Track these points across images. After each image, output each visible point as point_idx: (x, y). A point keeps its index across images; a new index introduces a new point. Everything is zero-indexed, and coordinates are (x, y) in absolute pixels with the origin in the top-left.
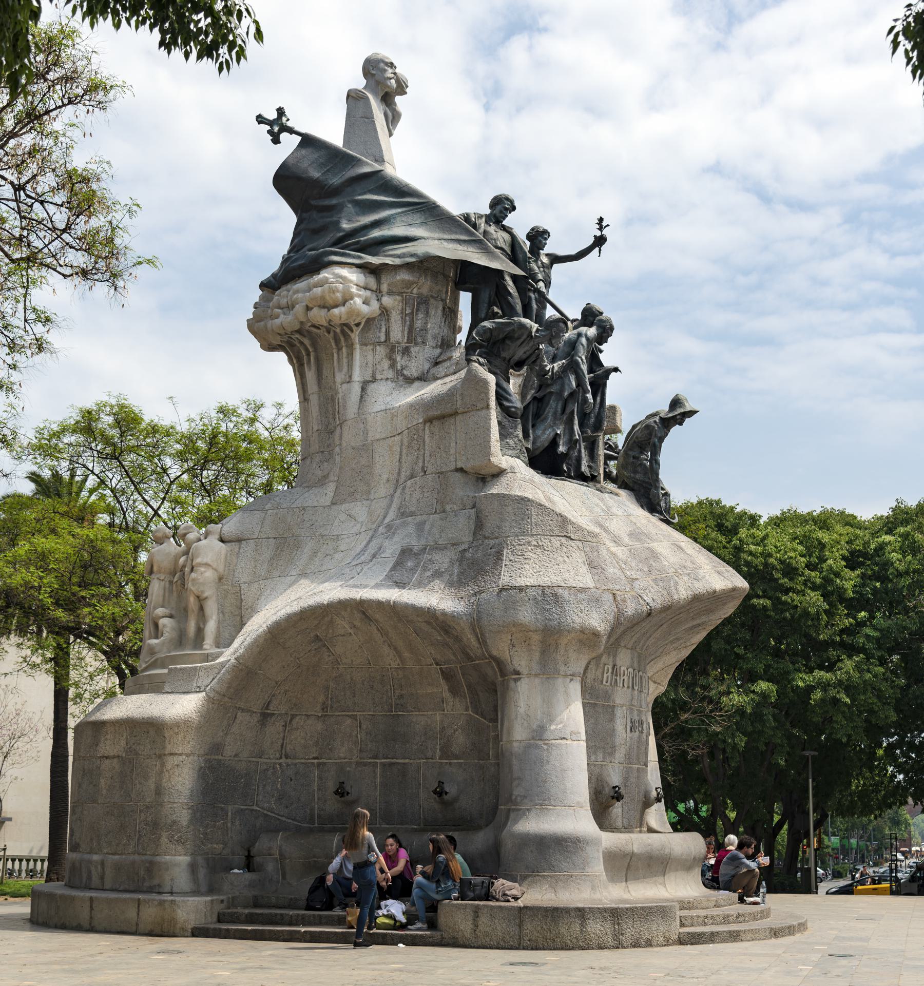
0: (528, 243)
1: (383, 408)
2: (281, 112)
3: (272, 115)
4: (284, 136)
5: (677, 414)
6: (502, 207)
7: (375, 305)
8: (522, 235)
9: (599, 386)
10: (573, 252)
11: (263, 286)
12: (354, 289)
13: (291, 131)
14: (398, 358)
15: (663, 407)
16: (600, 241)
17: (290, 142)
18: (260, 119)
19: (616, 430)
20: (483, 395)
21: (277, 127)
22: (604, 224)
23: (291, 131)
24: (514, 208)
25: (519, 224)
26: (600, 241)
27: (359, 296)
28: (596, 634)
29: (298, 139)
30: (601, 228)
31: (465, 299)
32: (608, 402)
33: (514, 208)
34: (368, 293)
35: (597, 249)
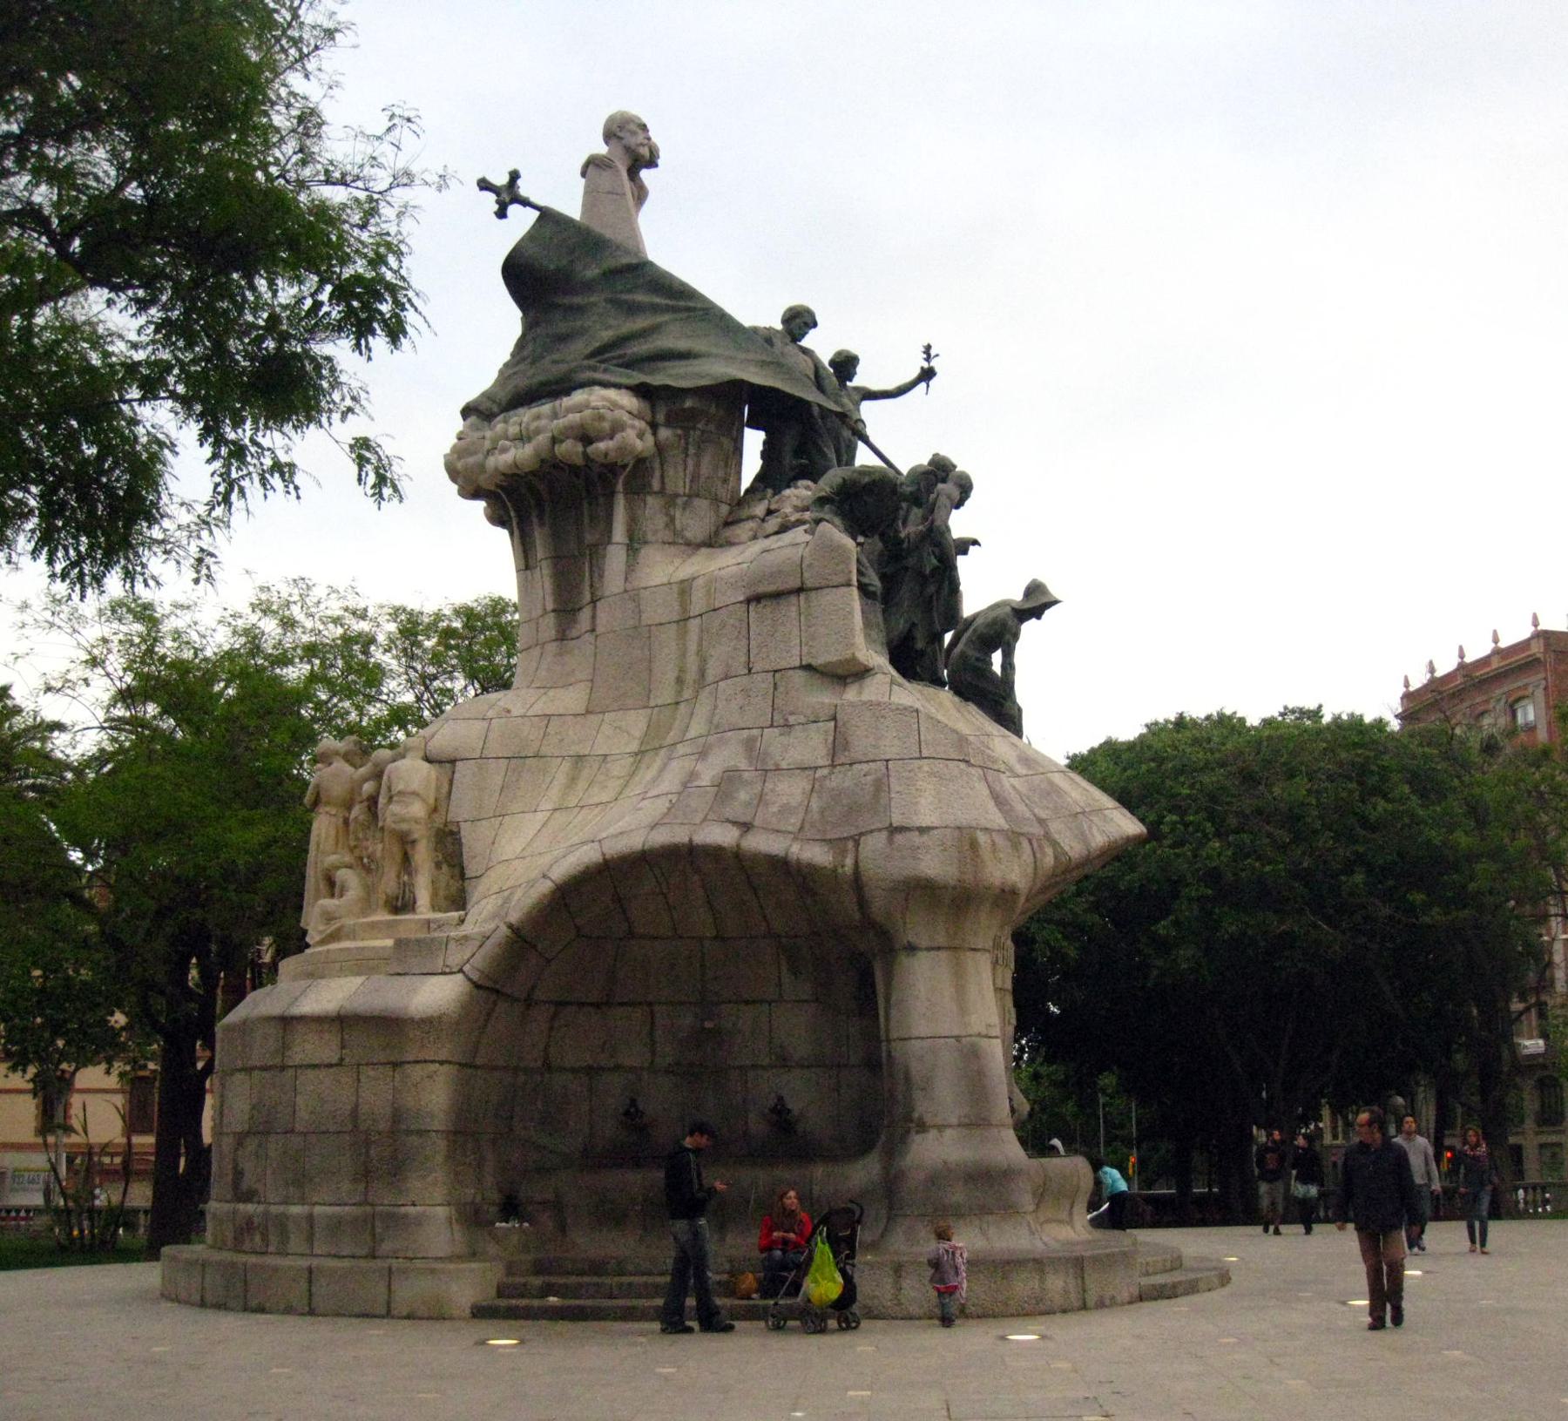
1: (665, 580)
2: (514, 176)
3: (501, 180)
4: (514, 209)
5: (1036, 603)
6: (799, 321)
7: (650, 439)
8: (825, 357)
10: (890, 385)
11: (467, 412)
12: (626, 417)
13: (525, 203)
15: (1016, 595)
16: (927, 375)
17: (521, 220)
18: (484, 185)
21: (507, 196)
22: (933, 353)
23: (525, 203)
24: (815, 325)
25: (822, 344)
26: (927, 375)
27: (633, 427)
28: (1014, 892)
29: (536, 214)
30: (928, 359)
31: (754, 441)
33: (815, 325)
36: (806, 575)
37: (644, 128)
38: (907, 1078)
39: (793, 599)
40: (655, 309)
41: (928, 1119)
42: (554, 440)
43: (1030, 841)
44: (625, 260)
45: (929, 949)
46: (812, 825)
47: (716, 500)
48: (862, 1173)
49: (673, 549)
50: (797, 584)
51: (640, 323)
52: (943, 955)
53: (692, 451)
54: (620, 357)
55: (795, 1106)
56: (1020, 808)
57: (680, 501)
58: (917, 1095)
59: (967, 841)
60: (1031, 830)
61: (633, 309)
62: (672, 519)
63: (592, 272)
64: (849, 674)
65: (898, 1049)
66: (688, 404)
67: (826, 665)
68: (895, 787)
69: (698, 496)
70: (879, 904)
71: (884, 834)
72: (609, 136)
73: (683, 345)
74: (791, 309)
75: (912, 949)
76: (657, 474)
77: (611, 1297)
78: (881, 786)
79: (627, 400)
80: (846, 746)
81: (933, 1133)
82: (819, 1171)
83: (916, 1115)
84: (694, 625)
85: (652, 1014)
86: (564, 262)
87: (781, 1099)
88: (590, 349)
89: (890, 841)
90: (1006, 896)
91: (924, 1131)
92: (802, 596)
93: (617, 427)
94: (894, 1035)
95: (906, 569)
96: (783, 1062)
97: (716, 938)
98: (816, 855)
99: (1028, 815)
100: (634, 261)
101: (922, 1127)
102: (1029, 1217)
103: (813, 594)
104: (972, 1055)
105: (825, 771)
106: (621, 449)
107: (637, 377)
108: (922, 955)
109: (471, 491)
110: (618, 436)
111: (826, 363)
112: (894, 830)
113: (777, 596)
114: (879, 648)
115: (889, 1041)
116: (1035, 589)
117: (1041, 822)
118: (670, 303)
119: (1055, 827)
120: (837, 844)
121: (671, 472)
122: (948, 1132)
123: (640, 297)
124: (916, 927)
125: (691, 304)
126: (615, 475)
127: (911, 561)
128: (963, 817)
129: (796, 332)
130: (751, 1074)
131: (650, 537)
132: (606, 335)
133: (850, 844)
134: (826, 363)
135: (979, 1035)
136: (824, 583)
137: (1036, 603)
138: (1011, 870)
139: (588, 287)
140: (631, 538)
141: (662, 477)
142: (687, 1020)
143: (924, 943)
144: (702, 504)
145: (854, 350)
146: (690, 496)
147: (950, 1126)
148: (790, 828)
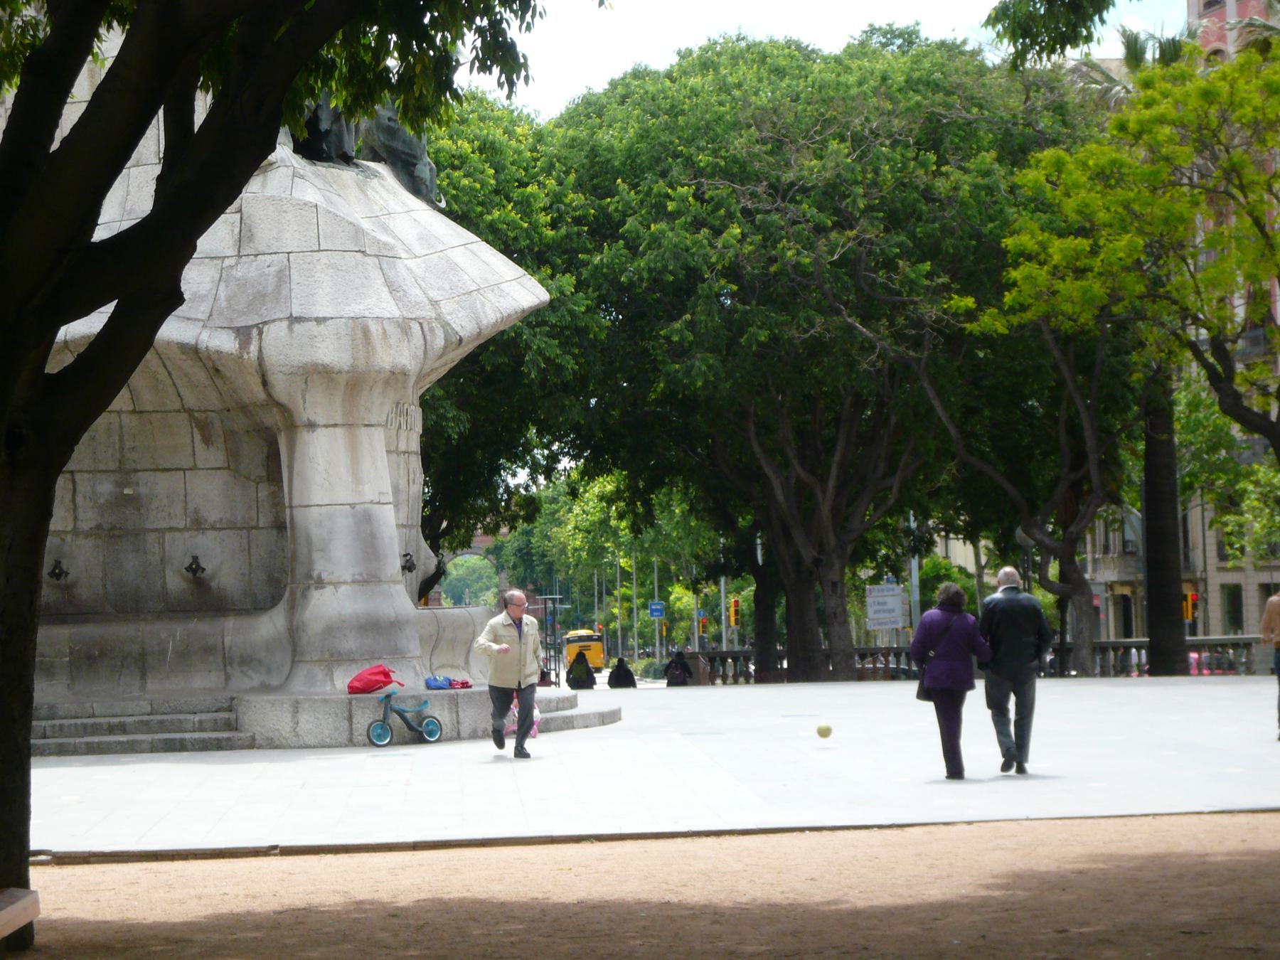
28: (405, 374)
38: (309, 542)
41: (324, 576)
43: (421, 324)
45: (327, 426)
46: (221, 314)
48: (270, 625)
52: (339, 431)
55: (208, 565)
56: (415, 293)
58: (316, 556)
59: (361, 331)
60: (423, 314)
65: (298, 513)
68: (295, 277)
70: (280, 389)
71: (285, 323)
75: (312, 426)
77: (45, 737)
78: (283, 277)
80: (251, 238)
81: (330, 589)
82: (230, 623)
83: (315, 574)
85: (74, 482)
87: (195, 559)
89: (290, 328)
90: (396, 377)
91: (322, 588)
94: (295, 503)
96: (198, 524)
97: (134, 412)
98: (225, 342)
99: (422, 298)
101: (320, 584)
102: (415, 662)
104: (364, 521)
105: (231, 262)
108: (319, 430)
112: (294, 320)
115: (291, 507)
117: (434, 303)
119: (446, 308)
120: (243, 334)
122: (343, 589)
124: (317, 406)
128: (355, 309)
130: (168, 536)
133: (255, 332)
135: (371, 502)
138: (402, 355)
142: (106, 487)
143: (321, 421)
147: (345, 583)
148: (200, 316)
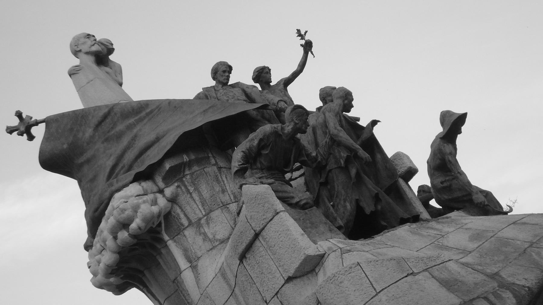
0: (258, 85)
1: (214, 275)
2: (19, 115)
3: (15, 122)
6: (222, 72)
9: (372, 145)
10: (294, 67)
14: (206, 230)
16: (308, 47)
17: (39, 131)
18: (10, 130)
19: (411, 172)
20: (266, 205)
21: (24, 127)
22: (303, 33)
23: (37, 123)
25: (243, 75)
26: (308, 47)
29: (44, 124)
32: (390, 153)
34: (150, 197)
35: (310, 53)
36: (253, 225)
37: (89, 36)
39: (257, 243)
40: (130, 127)
42: (115, 238)
43: (486, 299)
44: (101, 113)
47: (225, 206)
49: (214, 251)
50: (252, 233)
51: (125, 141)
53: (191, 189)
54: (122, 168)
57: (203, 221)
61: (119, 136)
62: (205, 234)
63: (89, 132)
64: (311, 266)
66: (167, 166)
67: (296, 271)
69: (211, 211)
72: (76, 53)
73: (152, 137)
74: (212, 70)
76: (182, 216)
79: (134, 188)
84: (237, 291)
86: (71, 139)
88: (106, 174)
92: (260, 238)
93: (136, 209)
95: (330, 171)
100: (106, 110)
103: (264, 233)
106: (147, 220)
107: (133, 173)
109: (119, 290)
110: (139, 214)
111: (251, 83)
113: (249, 247)
114: (329, 235)
116: (445, 116)
117: (494, 276)
118: (136, 118)
121: (188, 209)
123: (120, 127)
125: (148, 110)
126: (159, 233)
127: (331, 165)
129: (221, 79)
131: (199, 254)
132: (110, 163)
134: (252, 83)
136: (264, 222)
137: (453, 125)
139: (91, 141)
140: (190, 261)
141: (186, 215)
144: (217, 214)
145: (262, 65)
146: (207, 214)
